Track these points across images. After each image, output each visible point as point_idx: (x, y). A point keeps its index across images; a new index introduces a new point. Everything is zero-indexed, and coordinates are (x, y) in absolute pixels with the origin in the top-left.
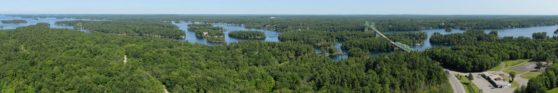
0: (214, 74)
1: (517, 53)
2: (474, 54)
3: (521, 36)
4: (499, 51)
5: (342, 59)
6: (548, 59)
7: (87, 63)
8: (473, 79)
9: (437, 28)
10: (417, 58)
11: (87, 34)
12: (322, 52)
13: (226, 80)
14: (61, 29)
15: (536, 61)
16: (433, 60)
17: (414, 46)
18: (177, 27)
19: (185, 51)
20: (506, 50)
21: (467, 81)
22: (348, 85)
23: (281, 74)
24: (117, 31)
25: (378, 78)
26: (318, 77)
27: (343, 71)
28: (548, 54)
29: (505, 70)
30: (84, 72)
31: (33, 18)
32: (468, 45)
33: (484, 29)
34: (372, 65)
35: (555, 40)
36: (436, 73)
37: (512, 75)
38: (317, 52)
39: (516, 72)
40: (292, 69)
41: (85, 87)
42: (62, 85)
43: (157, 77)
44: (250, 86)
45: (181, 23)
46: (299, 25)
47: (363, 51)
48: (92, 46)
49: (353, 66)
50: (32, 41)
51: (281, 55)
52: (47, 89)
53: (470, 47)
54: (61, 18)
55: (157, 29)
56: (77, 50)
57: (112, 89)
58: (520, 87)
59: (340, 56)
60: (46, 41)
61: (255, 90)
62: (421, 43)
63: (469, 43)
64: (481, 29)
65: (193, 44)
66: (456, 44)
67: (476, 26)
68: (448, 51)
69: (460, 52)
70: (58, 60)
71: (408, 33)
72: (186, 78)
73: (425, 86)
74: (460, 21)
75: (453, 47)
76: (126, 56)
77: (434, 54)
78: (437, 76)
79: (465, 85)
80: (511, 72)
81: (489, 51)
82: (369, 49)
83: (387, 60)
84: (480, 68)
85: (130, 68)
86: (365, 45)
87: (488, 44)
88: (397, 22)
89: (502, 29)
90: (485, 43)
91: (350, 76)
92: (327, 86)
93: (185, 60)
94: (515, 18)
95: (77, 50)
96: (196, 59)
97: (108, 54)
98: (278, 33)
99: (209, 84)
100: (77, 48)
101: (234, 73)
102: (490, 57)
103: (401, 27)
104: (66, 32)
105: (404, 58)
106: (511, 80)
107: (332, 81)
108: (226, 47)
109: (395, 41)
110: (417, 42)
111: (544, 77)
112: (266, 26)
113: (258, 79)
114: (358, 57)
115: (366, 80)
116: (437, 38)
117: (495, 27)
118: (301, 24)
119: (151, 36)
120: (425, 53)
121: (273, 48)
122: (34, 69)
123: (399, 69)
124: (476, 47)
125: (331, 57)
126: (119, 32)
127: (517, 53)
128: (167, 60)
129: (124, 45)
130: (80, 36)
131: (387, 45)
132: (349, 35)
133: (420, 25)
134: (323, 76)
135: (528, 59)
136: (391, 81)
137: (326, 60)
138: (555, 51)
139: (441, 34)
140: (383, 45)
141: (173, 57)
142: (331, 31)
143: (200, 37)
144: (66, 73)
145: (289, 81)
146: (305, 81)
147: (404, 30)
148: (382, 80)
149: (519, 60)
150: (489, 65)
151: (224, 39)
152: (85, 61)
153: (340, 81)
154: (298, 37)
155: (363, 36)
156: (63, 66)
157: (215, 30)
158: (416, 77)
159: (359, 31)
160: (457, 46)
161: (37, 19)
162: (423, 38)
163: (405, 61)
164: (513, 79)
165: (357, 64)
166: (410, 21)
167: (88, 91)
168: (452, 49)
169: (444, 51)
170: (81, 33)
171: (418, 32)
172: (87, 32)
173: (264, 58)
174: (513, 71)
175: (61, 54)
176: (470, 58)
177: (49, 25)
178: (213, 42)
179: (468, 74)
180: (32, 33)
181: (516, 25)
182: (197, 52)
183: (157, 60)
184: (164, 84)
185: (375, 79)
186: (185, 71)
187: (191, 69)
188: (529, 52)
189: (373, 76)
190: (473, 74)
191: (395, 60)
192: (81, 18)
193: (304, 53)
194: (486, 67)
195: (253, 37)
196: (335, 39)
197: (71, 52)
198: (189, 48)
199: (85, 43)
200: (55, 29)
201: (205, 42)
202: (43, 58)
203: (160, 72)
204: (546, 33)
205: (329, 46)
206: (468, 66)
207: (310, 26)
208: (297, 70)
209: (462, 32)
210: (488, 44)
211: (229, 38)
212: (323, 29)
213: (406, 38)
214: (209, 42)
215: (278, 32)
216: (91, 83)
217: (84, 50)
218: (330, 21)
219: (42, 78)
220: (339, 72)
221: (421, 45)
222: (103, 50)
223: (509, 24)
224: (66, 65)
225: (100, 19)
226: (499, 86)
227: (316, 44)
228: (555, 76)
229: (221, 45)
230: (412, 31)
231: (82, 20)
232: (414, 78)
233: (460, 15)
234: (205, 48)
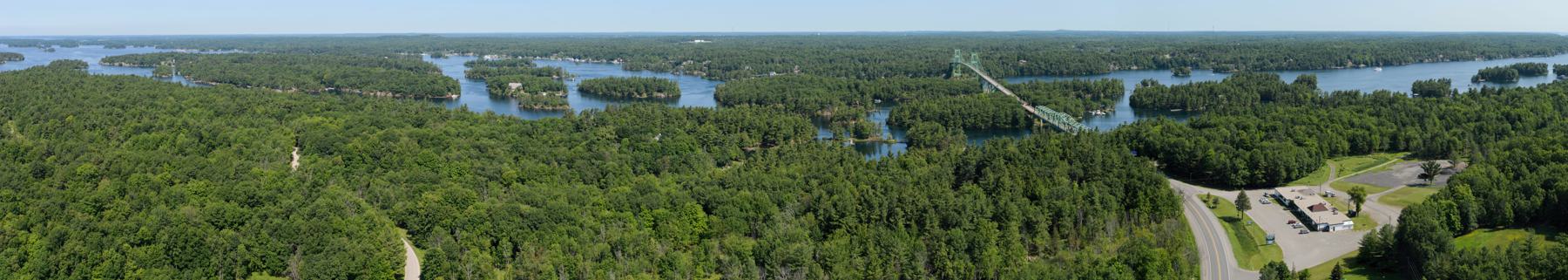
0: (539, 198)
1: (1370, 135)
2: (1252, 139)
3: (1380, 89)
4: (1322, 131)
5: (890, 155)
6: (1454, 152)
7: (190, 169)
8: (1249, 208)
9: (1150, 68)
10: (1097, 149)
11: (190, 90)
12: (835, 134)
13: (572, 215)
14: (117, 77)
15: (1424, 157)
16: (1138, 155)
17: (1088, 117)
18: (435, 69)
19: (458, 136)
20: (1340, 127)
21: (1234, 213)
22: (907, 226)
23: (724, 194)
24: (271, 82)
25: (988, 206)
26: (826, 203)
27: (892, 187)
28: (1456, 138)
29: (1338, 182)
30: (182, 196)
31: (40, 47)
32: (1236, 113)
33: (1280, 69)
35: (1475, 99)
36: (1148, 191)
37: (1357, 197)
38: (822, 135)
39: (1366, 187)
40: (753, 183)
41: (183, 236)
42: (121, 231)
43: (383, 208)
44: (639, 228)
45: (447, 58)
46: (773, 61)
47: (947, 130)
48: (203, 123)
49: (920, 174)
50: (39, 109)
51: (722, 144)
52: (82, 242)
53: (1242, 119)
54: (118, 47)
55: (383, 76)
56: (162, 134)
57: (260, 242)
58: (1378, 229)
59: (885, 148)
60: (78, 109)
61: (652, 239)
63: (1238, 108)
64: (1271, 69)
65: (481, 115)
67: (1256, 63)
68: (1181, 132)
69: (1213, 132)
70: (111, 163)
71: (1070, 80)
72: (461, 209)
73: (1118, 227)
74: (1212, 48)
75: (1194, 119)
76: (297, 149)
77: (1140, 141)
78: (1151, 200)
79: (1227, 224)
80: (1353, 189)
82: (964, 126)
83: (1012, 157)
84: (1271, 179)
85: (308, 184)
86: (953, 114)
87: (1290, 112)
88: (1040, 53)
89: (1331, 69)
90: (1282, 109)
91: (913, 201)
92: (850, 227)
93: (459, 159)
94: (1364, 40)
95: (162, 134)
96: (488, 157)
97: (247, 145)
98: (715, 83)
99: (525, 226)
100: (161, 128)
101: (594, 195)
102: (1296, 149)
103: (1051, 65)
104: (132, 85)
105: (1061, 151)
106: (1355, 210)
107: (862, 215)
109: (1034, 105)
110: (1095, 107)
111: (1443, 202)
112: (680, 63)
113: (661, 210)
114: (935, 149)
115: (955, 210)
116: (1151, 95)
117: (1308, 63)
118: (777, 58)
119: (364, 93)
120: (1117, 136)
121: (701, 123)
122: (43, 187)
123: (1048, 180)
124: (1258, 120)
125: (862, 148)
126: (279, 83)
127: (1370, 135)
128: (408, 160)
129: (292, 119)
130: (170, 94)
131: (1015, 115)
132: (908, 89)
133: (1103, 58)
134: (839, 200)
135: (1400, 151)
136: (1023, 215)
137: (846, 156)
139: (1161, 83)
140: (1003, 115)
141: (425, 151)
142: (859, 77)
143: (499, 94)
144: (132, 198)
145: (744, 214)
146: (789, 214)
147: (1061, 74)
148: (1001, 211)
149: (1376, 155)
150: (1294, 170)
151: (565, 100)
152: (184, 163)
153: (885, 215)
154: (769, 94)
155: (946, 90)
156: (125, 177)
157: (540, 75)
158: (1092, 202)
159: (936, 78)
160: (1204, 118)
161: (53, 50)
162: (1111, 94)
163: (1061, 159)
164: (1358, 209)
165: (932, 167)
166: (1078, 49)
167: (192, 247)
168: (1191, 124)
169: (1169, 130)
170: (171, 86)
171: (1099, 79)
172: (191, 85)
173: (677, 153)
174: (1360, 186)
175: (118, 146)
176: (1240, 150)
177: (86, 65)
178: (536, 111)
179: (1232, 196)
180: (37, 88)
181: (1367, 59)
182: (491, 137)
183: (383, 159)
184: (402, 225)
185: (982, 210)
186: (460, 188)
187: (476, 185)
188: (1403, 133)
189: (975, 199)
190: (1249, 193)
191: (1034, 155)
192: (172, 47)
193: (785, 139)
194: (1284, 174)
195: (645, 96)
196: (871, 99)
197: (146, 141)
198: (470, 127)
199: (185, 115)
200: (102, 77)
201: (512, 110)
202: (68, 157)
203: (391, 192)
204: (1449, 82)
205: (855, 119)
206: (1235, 170)
207: (800, 64)
208: (767, 183)
209: (1218, 78)
210: (1290, 112)
211: (580, 97)
212: (838, 71)
213: (1066, 95)
214: (526, 109)
215: (715, 80)
216: (200, 224)
217: (181, 134)
218: (855, 49)
219: (65, 211)
220: (883, 190)
221: (1107, 115)
222: (235, 135)
223: (1349, 58)
224: (133, 175)
225: (224, 49)
226: (1322, 227)
227: (819, 112)
228: (1473, 198)
229: (559, 117)
230: (1081, 75)
231: (174, 51)
232: (1088, 205)
233: (1213, 32)
234: (514, 126)
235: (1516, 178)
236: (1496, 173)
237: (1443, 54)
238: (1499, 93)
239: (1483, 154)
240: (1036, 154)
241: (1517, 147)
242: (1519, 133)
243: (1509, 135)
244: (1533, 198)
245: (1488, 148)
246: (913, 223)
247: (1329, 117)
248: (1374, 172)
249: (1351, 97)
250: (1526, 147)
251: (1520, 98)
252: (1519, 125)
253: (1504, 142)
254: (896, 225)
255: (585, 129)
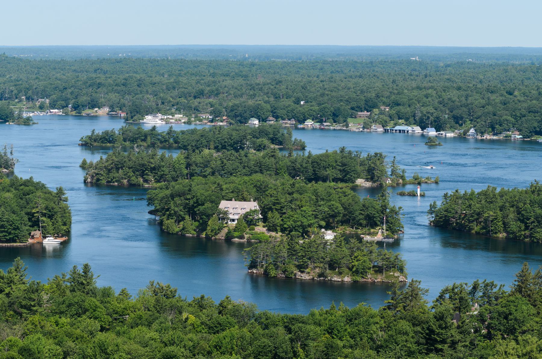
65: (133, 300)
108: (415, 322)
157: (316, 178)
178: (303, 284)
198: (101, 336)
211: (438, 246)
234: (235, 331)
255: (453, 344)
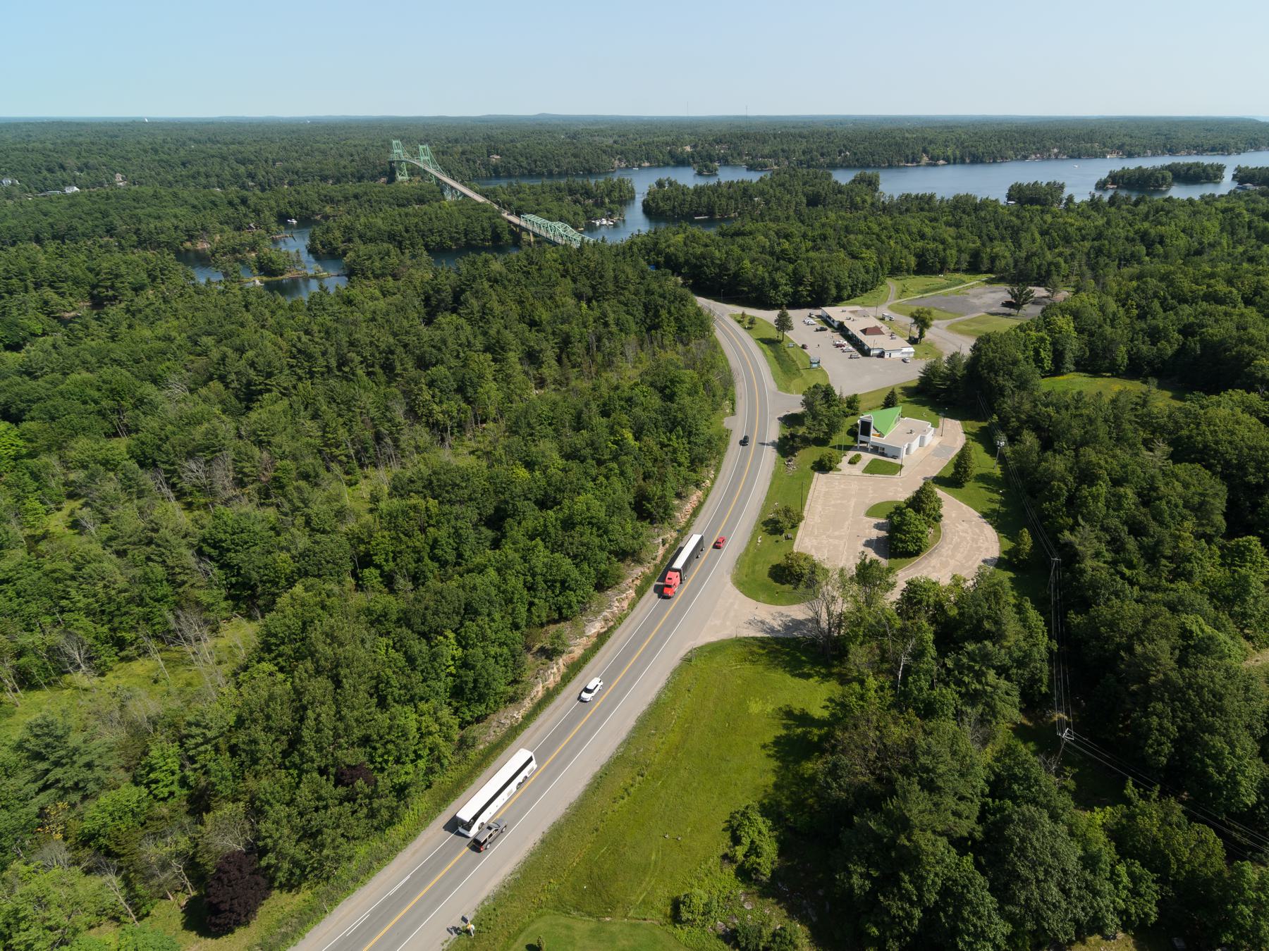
1: (944, 250)
3: (963, 193)
6: (1055, 277)
15: (1013, 281)
22: (369, 374)
28: (1061, 260)
34: (449, 299)
39: (935, 312)
53: (783, 225)
62: (615, 219)
66: (735, 218)
75: (724, 225)
81: (849, 242)
87: (843, 218)
91: (371, 342)
94: (948, 127)
116: (669, 199)
124: (803, 228)
127: (944, 250)
138: (1088, 254)
139: (681, 182)
149: (949, 275)
154: (76, 223)
160: (737, 225)
162: (621, 198)
165: (390, 299)
181: (949, 152)
204: (1062, 187)
210: (843, 218)
213: (560, 199)
221: (615, 226)
228: (1074, 334)
235: (1142, 317)
236: (1112, 306)
237: (1059, 148)
238: (1136, 204)
239: (1097, 282)
240: (529, 273)
241: (1152, 277)
242: (1156, 260)
243: (1140, 262)
244: (1162, 344)
245: (1105, 275)
246: (377, 369)
247: (893, 226)
248: (944, 295)
249: (924, 203)
250: (1164, 278)
251: (1168, 212)
252: (1159, 249)
253: (1135, 269)
254: (354, 374)
